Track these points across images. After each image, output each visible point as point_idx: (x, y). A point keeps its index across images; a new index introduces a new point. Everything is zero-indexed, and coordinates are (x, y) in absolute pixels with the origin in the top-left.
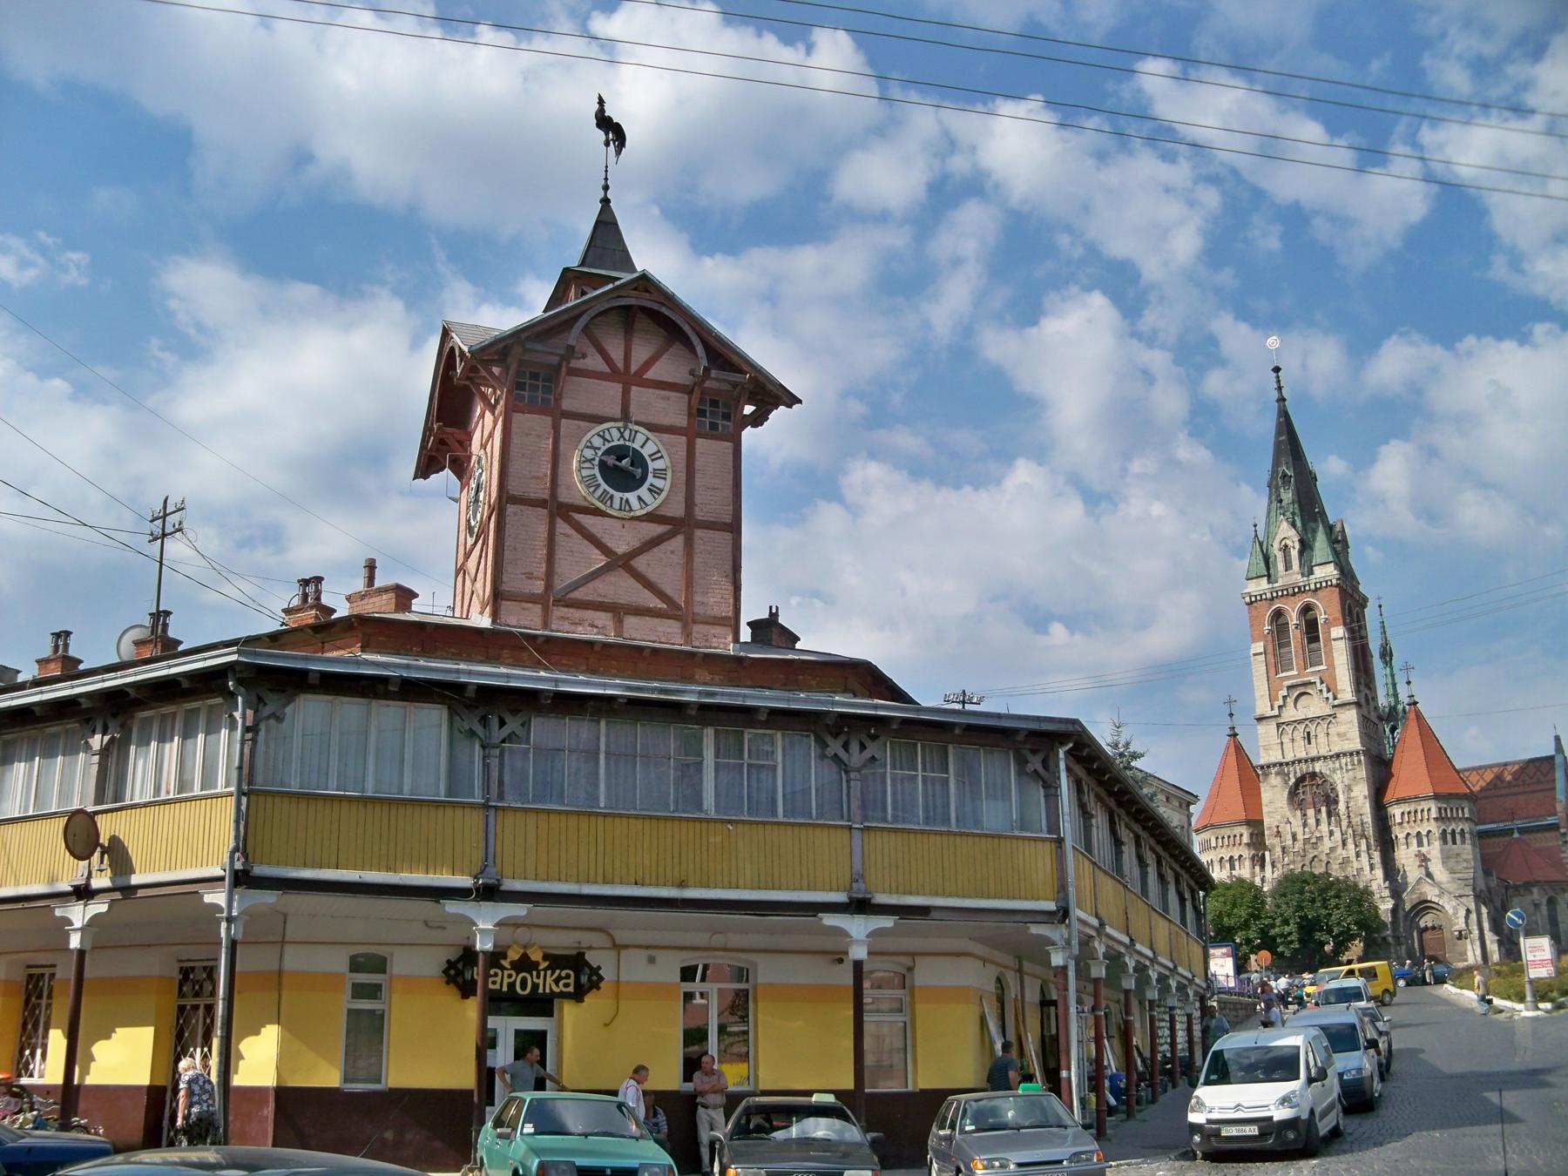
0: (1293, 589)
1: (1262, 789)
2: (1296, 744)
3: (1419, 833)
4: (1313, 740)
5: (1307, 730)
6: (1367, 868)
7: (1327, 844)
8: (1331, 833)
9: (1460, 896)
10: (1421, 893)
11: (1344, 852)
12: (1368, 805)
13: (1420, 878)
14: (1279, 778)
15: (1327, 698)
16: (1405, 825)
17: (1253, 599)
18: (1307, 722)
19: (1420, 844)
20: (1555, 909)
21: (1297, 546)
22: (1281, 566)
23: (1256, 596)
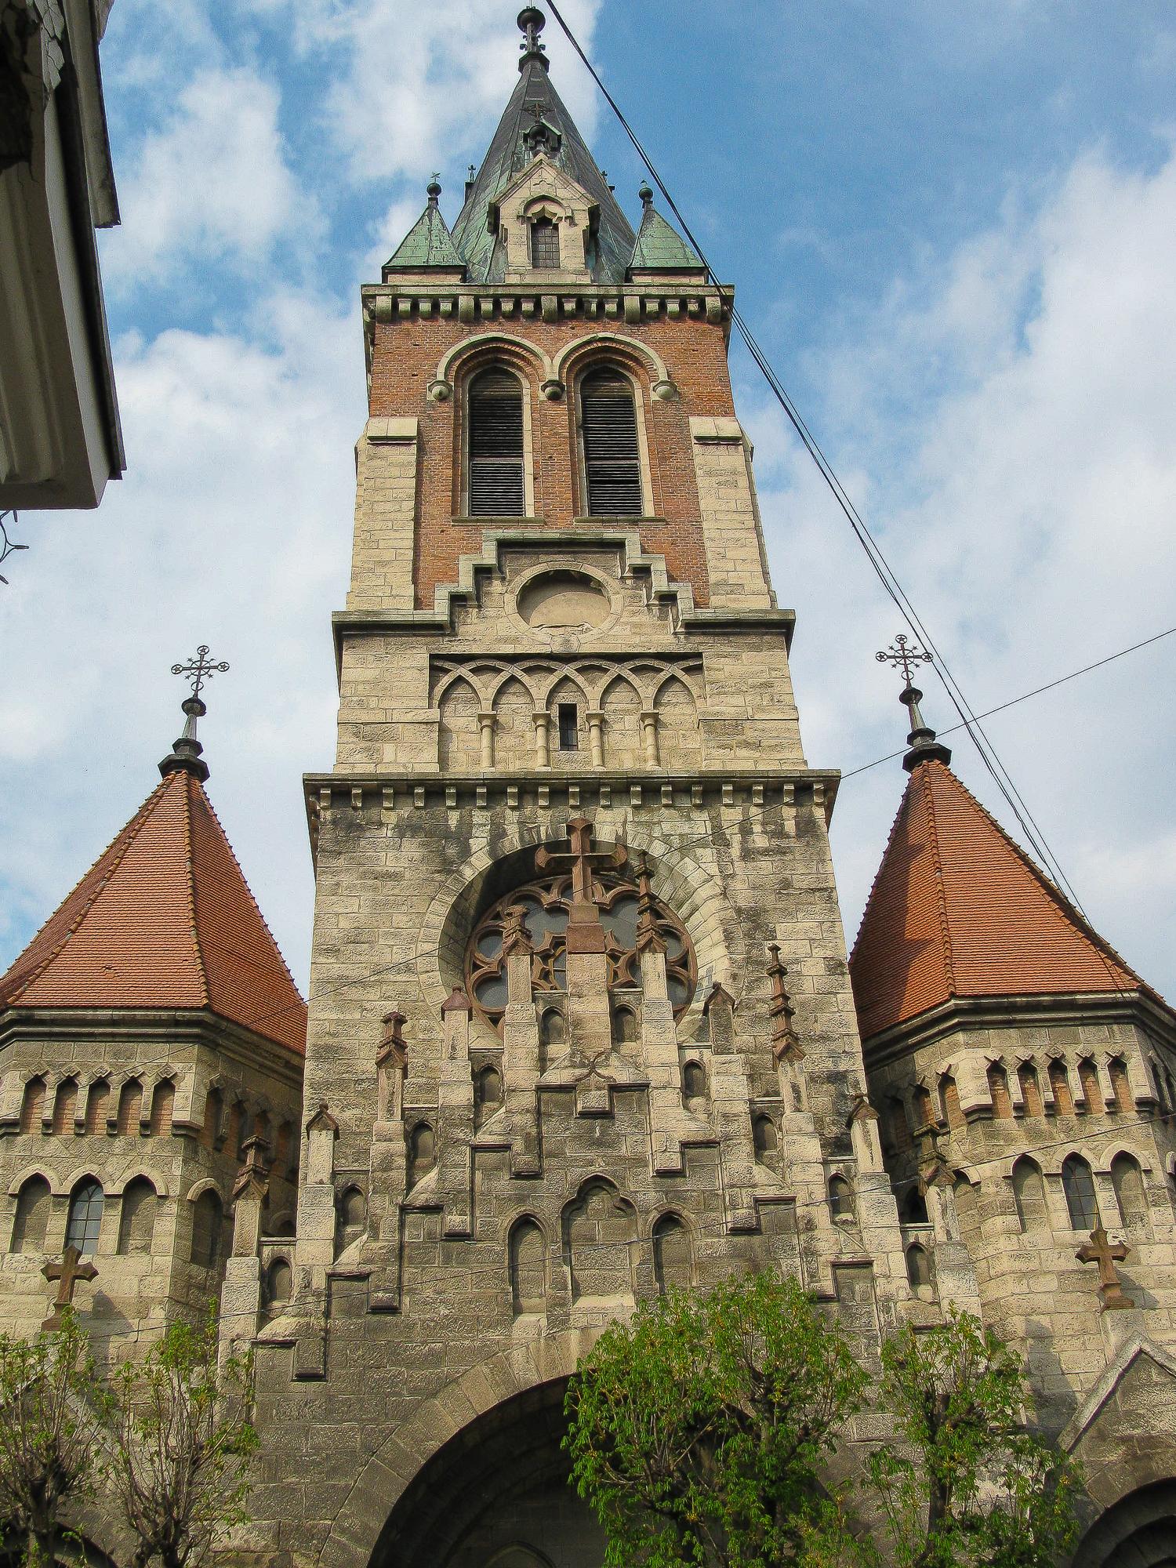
0: (560, 297)
3: (1075, 1161)
4: (588, 738)
5: (565, 697)
8: (692, 1080)
11: (760, 1173)
12: (847, 997)
14: (412, 849)
15: (668, 599)
16: (1007, 1121)
17: (405, 306)
18: (569, 670)
21: (583, 221)
22: (518, 253)
23: (415, 301)
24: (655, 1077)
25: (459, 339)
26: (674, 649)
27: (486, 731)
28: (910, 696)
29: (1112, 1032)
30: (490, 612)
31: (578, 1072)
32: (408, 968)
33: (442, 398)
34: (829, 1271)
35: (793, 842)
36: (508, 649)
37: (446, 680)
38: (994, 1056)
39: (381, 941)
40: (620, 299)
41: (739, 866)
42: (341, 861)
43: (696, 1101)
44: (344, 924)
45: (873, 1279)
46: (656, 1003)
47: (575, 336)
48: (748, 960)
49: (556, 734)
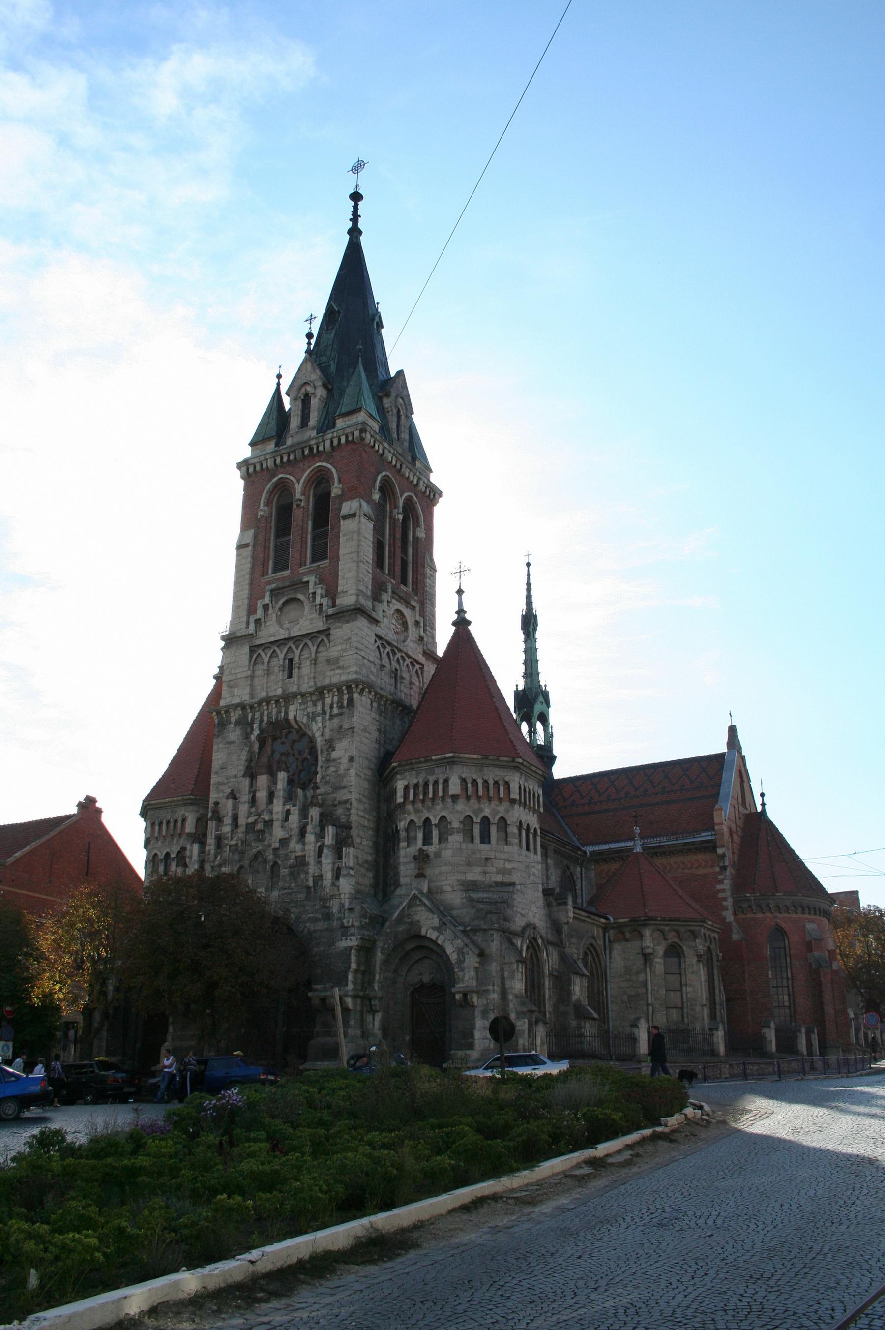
1: (215, 747)
2: (273, 677)
4: (295, 672)
5: (290, 656)
6: (328, 876)
7: (278, 832)
9: (475, 930)
10: (412, 923)
11: (299, 847)
12: (353, 772)
13: (415, 897)
14: (238, 732)
15: (321, 605)
16: (409, 807)
17: (251, 470)
18: (291, 644)
19: (427, 840)
20: (680, 963)
21: (321, 392)
24: (275, 817)
25: (270, 480)
26: (321, 628)
27: (266, 676)
28: (460, 592)
29: (446, 769)
30: (268, 623)
31: (256, 817)
32: (236, 776)
33: (262, 517)
34: (311, 879)
35: (345, 710)
36: (272, 639)
37: (255, 656)
38: (406, 784)
39: (229, 767)
40: (324, 441)
41: (328, 722)
42: (220, 740)
43: (286, 824)
44: (220, 763)
45: (322, 880)
46: (280, 790)
47: (309, 467)
48: (328, 761)
49: (286, 673)
